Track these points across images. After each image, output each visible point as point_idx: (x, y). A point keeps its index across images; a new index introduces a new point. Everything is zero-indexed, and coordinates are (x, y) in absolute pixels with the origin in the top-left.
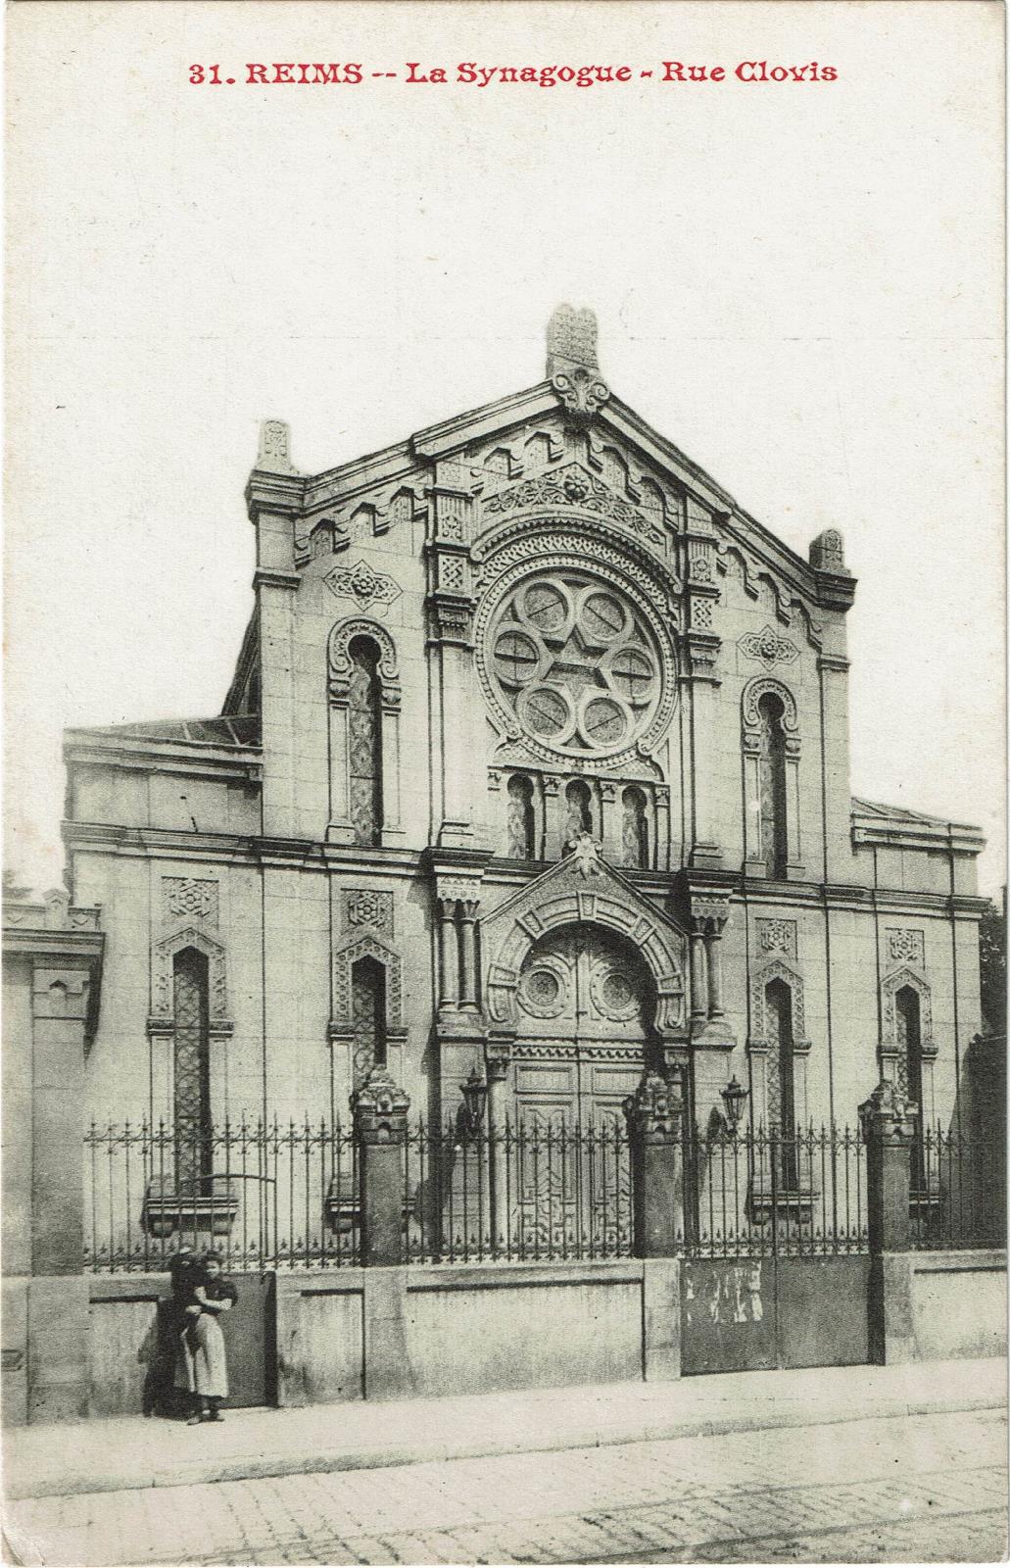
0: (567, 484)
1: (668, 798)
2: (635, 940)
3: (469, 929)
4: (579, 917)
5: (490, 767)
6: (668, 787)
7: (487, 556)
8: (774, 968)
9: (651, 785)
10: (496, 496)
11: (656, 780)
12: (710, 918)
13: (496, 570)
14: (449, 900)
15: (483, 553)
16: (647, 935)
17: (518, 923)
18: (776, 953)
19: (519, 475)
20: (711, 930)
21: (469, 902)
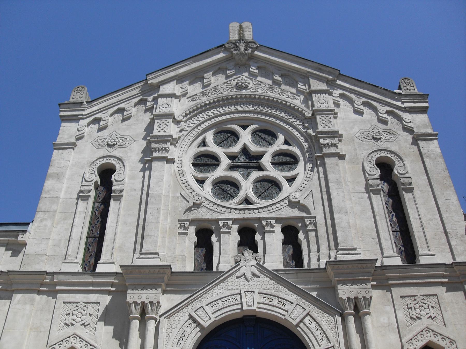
0: (237, 83)
1: (315, 225)
2: (291, 320)
3: (151, 325)
4: (242, 308)
5: (179, 221)
6: (315, 217)
7: (185, 119)
8: (425, 333)
9: (302, 219)
10: (196, 95)
11: (305, 215)
12: (356, 298)
13: (192, 123)
14: (135, 303)
15: (184, 117)
16: (302, 316)
17: (191, 317)
18: (425, 322)
19: (209, 85)
20: (359, 308)
21: (151, 303)
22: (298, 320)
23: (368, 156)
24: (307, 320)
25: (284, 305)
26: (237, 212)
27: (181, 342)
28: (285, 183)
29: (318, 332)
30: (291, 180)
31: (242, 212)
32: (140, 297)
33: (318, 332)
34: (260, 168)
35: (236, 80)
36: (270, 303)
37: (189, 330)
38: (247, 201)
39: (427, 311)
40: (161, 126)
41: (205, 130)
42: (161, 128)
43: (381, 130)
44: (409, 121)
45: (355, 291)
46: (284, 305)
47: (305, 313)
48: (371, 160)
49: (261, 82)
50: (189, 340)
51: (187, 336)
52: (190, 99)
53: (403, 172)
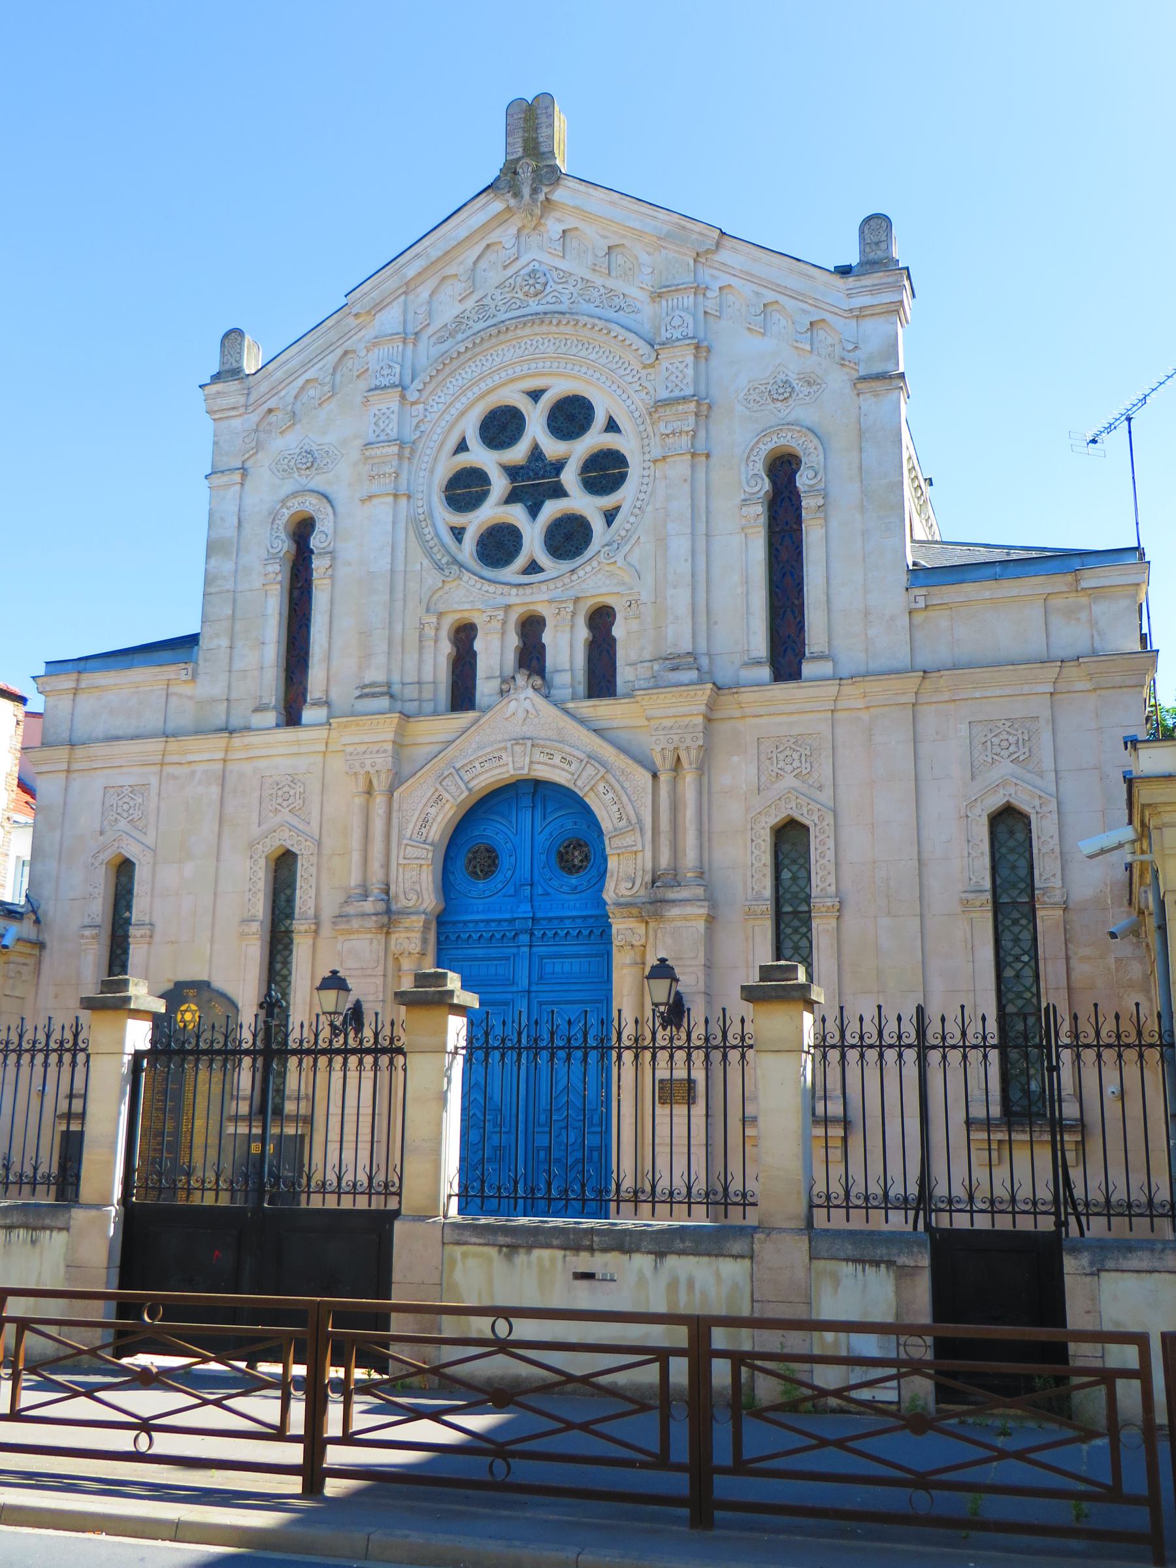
12: (676, 749)
18: (789, 781)
22: (587, 788)
23: (752, 450)
24: (601, 788)
25: (570, 763)
26: (514, 591)
27: (423, 830)
28: (597, 524)
29: (615, 808)
30: (610, 516)
31: (521, 590)
32: (363, 765)
33: (615, 808)
34: (559, 492)
35: (522, 273)
36: (550, 761)
37: (433, 811)
38: (533, 568)
39: (796, 764)
40: (380, 423)
41: (463, 413)
42: (382, 426)
43: (792, 377)
44: (851, 347)
45: (676, 738)
46: (570, 763)
47: (599, 776)
48: (756, 459)
49: (571, 274)
50: (434, 828)
51: (431, 820)
52: (433, 339)
53: (812, 482)
